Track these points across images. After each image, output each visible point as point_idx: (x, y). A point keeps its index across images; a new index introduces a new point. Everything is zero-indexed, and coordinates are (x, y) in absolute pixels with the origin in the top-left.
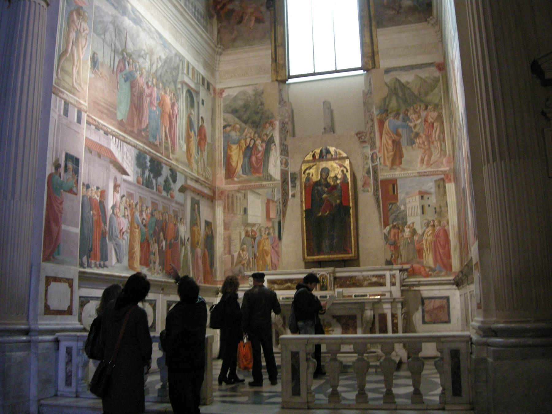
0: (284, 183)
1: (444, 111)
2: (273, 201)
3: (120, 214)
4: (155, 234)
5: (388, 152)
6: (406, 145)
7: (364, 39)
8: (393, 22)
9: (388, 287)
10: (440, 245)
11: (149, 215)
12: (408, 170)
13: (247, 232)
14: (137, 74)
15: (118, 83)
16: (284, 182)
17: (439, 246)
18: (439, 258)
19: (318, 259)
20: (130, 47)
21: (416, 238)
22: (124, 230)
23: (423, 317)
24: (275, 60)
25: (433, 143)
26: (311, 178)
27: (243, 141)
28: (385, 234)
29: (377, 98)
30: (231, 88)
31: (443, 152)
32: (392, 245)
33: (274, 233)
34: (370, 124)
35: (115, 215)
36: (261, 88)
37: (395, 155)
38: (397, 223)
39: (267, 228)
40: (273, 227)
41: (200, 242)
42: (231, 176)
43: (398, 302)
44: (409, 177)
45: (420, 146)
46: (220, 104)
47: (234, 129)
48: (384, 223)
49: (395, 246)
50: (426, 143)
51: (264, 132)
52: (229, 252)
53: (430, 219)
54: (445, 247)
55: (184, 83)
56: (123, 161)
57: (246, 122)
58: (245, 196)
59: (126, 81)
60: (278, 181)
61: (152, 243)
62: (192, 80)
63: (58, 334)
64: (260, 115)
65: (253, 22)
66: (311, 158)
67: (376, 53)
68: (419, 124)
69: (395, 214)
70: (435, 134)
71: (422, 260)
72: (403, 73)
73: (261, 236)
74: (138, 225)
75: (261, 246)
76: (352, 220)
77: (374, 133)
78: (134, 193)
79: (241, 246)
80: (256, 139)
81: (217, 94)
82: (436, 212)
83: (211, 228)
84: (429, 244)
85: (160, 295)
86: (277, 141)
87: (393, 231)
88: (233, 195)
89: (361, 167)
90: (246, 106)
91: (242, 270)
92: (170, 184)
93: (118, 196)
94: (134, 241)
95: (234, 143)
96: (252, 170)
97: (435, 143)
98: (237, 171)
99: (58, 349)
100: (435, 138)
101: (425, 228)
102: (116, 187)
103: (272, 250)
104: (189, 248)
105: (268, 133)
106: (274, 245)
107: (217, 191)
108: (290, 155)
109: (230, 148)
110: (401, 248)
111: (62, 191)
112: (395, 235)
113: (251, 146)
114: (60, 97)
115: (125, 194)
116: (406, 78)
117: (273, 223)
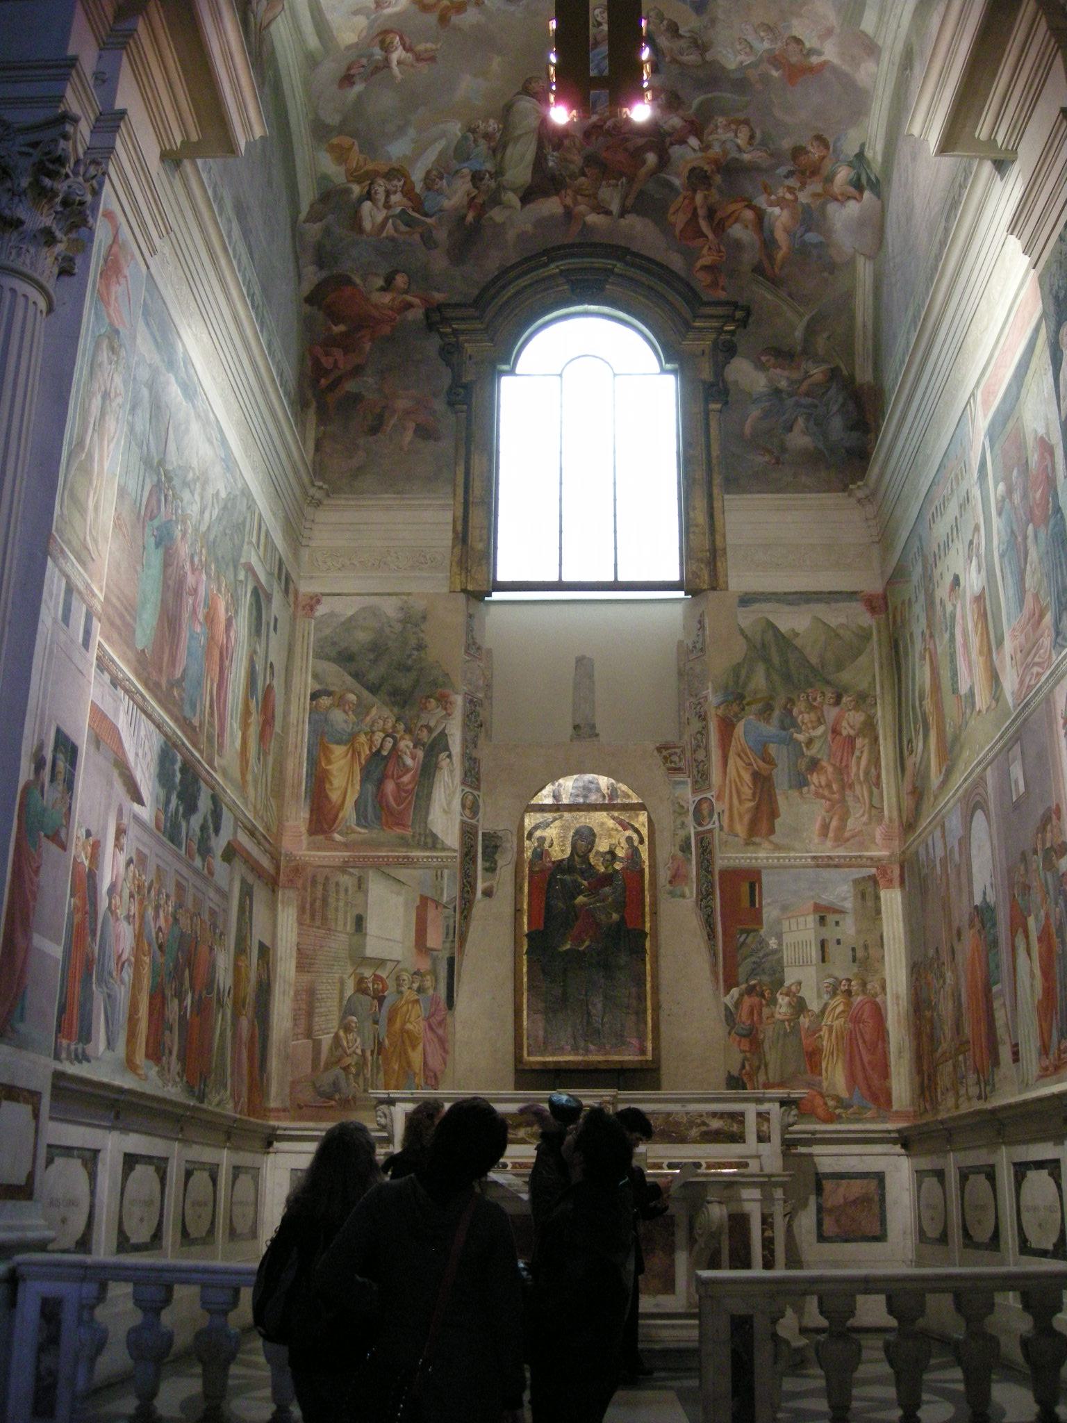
1: (879, 714)
2: (437, 904)
3: (121, 913)
4: (176, 974)
5: (740, 801)
6: (786, 787)
7: (692, 515)
8: (762, 482)
9: (751, 1145)
10: (864, 1042)
11: (171, 919)
12: (789, 848)
13: (361, 981)
14: (178, 534)
15: (144, 548)
17: (861, 1045)
18: (860, 1076)
20: (173, 460)
21: (805, 1021)
22: (125, 957)
23: (820, 1224)
24: (462, 537)
25: (851, 786)
28: (727, 1008)
29: (720, 662)
31: (875, 810)
33: (435, 989)
34: (696, 725)
37: (757, 808)
38: (760, 981)
42: (325, 826)
43: (776, 1185)
44: (792, 867)
45: (821, 791)
46: (309, 633)
47: (341, 703)
48: (725, 981)
49: (752, 1038)
50: (835, 787)
52: (309, 1034)
53: (841, 974)
54: (877, 1046)
55: (250, 569)
56: (136, 764)
57: (374, 689)
58: (361, 884)
59: (157, 545)
60: (455, 851)
62: (262, 561)
63: (20, 1258)
64: (413, 675)
65: (409, 435)
67: (719, 553)
68: (821, 737)
69: (754, 959)
70: (858, 765)
71: (819, 1078)
72: (787, 609)
73: (401, 993)
74: (150, 945)
75: (398, 1020)
77: (707, 748)
79: (343, 1018)
80: (398, 736)
81: (300, 608)
82: (854, 961)
83: (268, 964)
84: (837, 1037)
85: (225, 1152)
86: (456, 746)
87: (747, 1001)
88: (327, 878)
90: (377, 649)
91: (343, 1084)
92: (209, 838)
93: (122, 859)
94: (140, 990)
95: (339, 742)
97: (857, 787)
98: (341, 815)
99: (12, 1303)
100: (857, 775)
101: (826, 997)
102: (120, 832)
103: (430, 1034)
104: (229, 1012)
105: (432, 724)
106: (433, 1021)
107: (283, 864)
108: (483, 786)
109: (327, 751)
110: (767, 1045)
111: (42, 834)
112: (751, 1013)
113: (385, 753)
114: (61, 570)
116: (792, 621)
117: (435, 961)
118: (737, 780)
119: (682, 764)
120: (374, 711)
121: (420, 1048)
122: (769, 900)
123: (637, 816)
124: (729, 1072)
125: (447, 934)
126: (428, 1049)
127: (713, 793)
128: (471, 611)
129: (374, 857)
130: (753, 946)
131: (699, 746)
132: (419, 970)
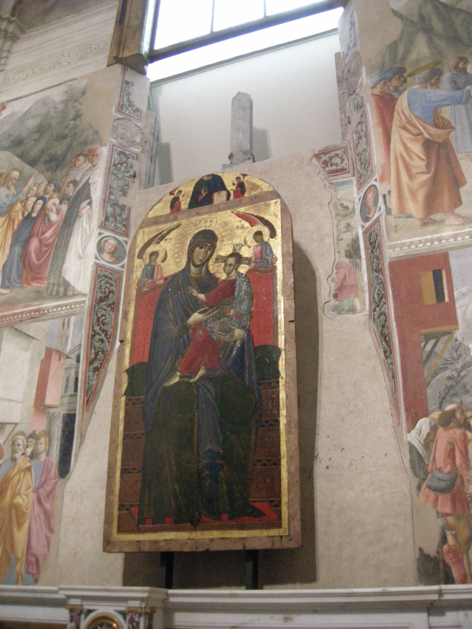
0: (103, 305)
5: (411, 176)
16: (101, 300)
19: (156, 542)
24: (121, 20)
26: (159, 266)
27: (19, 207)
30: (21, 98)
32: (442, 491)
34: (355, 117)
36: (83, 84)
37: (435, 180)
39: (32, 435)
40: (48, 434)
48: (407, 410)
51: (71, 179)
57: (33, 163)
60: (84, 295)
66: (168, 210)
69: (448, 373)
73: (14, 460)
76: (282, 395)
80: (47, 196)
89: (329, 241)
90: (41, 129)
96: (24, 276)
105: (78, 179)
112: (451, 454)
113: (34, 215)
117: (51, 419)
118: (404, 154)
119: (344, 165)
120: (31, 181)
121: (26, 526)
122: (464, 290)
123: (268, 206)
124: (421, 550)
125: (67, 387)
126: (34, 528)
127: (376, 176)
128: (128, 78)
129: (9, 316)
130: (446, 355)
131: (360, 138)
132: (34, 432)
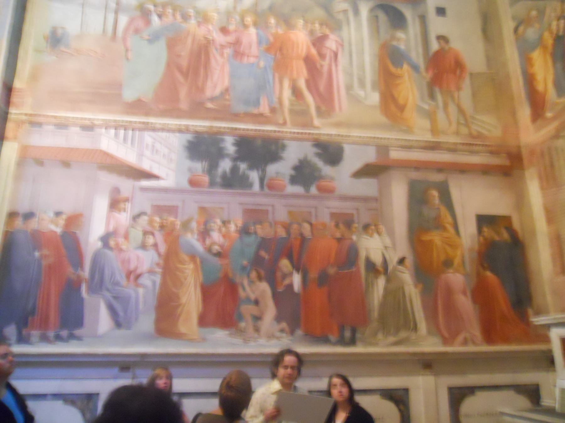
15: (127, 50)
27: (546, 35)
35: (110, 248)
41: (457, 261)
61: (246, 282)
78: (180, 204)
95: (534, 49)
98: (547, 97)
107: (525, 153)
115: (148, 210)
120: (548, 11)
